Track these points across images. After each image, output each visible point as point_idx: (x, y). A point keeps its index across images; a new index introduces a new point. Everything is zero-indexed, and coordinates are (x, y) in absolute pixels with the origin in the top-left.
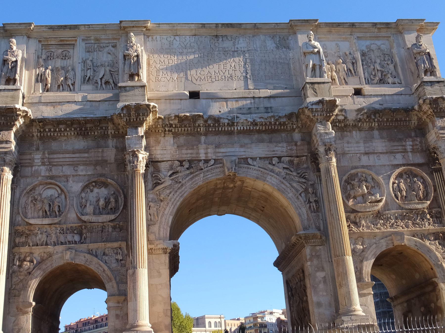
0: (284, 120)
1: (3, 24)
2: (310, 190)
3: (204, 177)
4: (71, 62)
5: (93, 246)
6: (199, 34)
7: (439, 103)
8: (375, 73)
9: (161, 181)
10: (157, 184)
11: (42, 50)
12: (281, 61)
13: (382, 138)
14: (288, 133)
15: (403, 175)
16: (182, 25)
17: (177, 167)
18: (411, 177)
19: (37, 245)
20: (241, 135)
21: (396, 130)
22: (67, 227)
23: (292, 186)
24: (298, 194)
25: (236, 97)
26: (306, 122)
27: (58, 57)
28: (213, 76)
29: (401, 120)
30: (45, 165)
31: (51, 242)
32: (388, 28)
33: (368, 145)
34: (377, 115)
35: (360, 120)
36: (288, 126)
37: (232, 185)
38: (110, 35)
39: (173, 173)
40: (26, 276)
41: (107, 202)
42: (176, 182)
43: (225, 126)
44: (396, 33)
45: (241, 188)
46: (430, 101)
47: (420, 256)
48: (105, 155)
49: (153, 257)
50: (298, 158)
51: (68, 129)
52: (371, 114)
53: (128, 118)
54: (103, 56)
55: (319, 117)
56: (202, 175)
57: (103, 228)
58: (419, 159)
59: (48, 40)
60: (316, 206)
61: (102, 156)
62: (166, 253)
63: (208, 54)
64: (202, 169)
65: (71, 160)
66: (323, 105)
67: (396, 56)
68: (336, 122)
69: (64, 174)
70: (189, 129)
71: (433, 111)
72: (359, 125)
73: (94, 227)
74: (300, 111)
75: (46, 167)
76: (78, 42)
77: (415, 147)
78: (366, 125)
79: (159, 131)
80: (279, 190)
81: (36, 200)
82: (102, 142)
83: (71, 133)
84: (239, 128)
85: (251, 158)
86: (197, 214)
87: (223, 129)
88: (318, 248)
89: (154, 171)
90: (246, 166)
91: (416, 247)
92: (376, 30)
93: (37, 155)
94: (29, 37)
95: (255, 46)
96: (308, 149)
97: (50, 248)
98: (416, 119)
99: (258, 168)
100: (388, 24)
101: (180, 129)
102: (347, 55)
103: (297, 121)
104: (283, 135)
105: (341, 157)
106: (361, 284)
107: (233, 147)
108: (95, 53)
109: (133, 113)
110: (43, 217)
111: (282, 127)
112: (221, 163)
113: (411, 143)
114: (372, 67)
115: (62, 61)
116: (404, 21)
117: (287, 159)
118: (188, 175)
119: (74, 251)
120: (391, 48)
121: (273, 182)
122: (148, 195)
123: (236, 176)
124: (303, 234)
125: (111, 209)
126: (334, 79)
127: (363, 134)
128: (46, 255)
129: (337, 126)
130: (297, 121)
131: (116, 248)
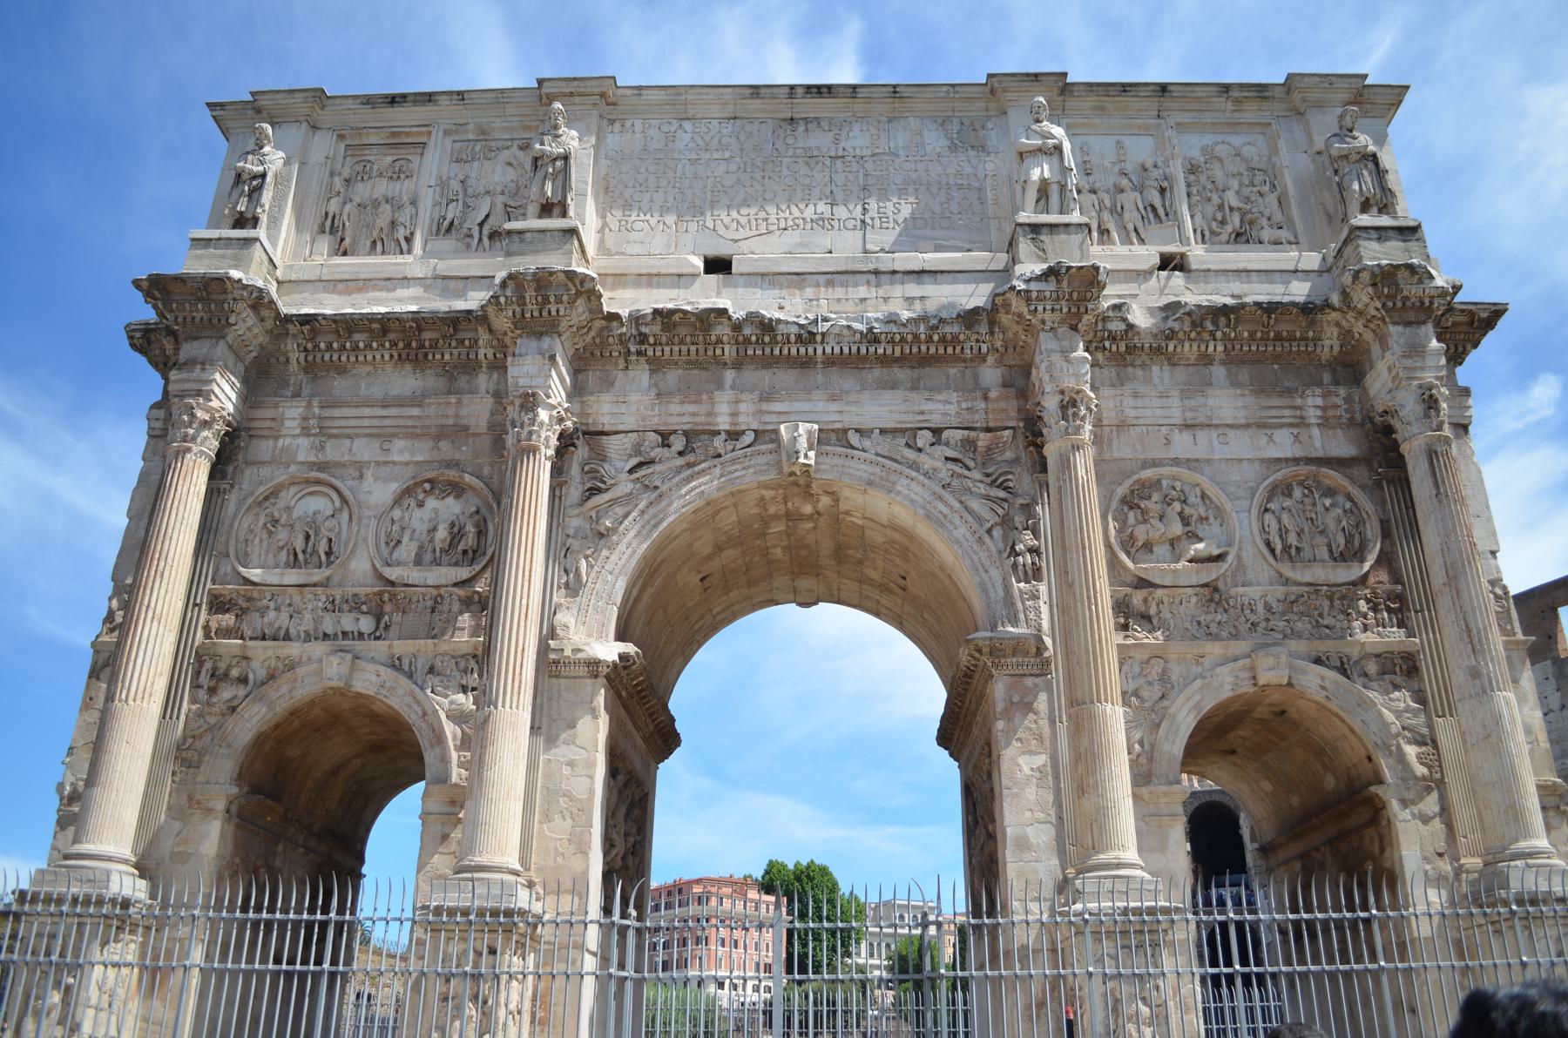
0: (956, 329)
1: (253, 94)
2: (1019, 520)
3: (722, 476)
4: (413, 186)
5: (402, 647)
6: (744, 115)
7: (1401, 282)
8: (1224, 217)
9: (605, 483)
10: (594, 491)
11: (344, 158)
12: (960, 182)
13: (1235, 383)
15: (1293, 489)
16: (700, 90)
17: (652, 448)
18: (1317, 496)
19: (264, 639)
20: (835, 370)
21: (1276, 367)
22: (343, 597)
23: (966, 508)
24: (982, 531)
25: (827, 270)
26: (1016, 334)
27: (380, 175)
28: (773, 219)
29: (1292, 338)
30: (309, 435)
31: (298, 632)
32: (1265, 98)
33: (1193, 403)
34: (1222, 320)
35: (1171, 335)
36: (967, 346)
38: (515, 119)
39: (640, 465)
40: (224, 715)
41: (456, 533)
42: (647, 486)
43: (789, 342)
45: (837, 518)
46: (1373, 275)
47: (1335, 719)
48: (464, 412)
51: (375, 345)
52: (1203, 320)
53: (518, 309)
54: (493, 171)
55: (1048, 316)
56: (717, 471)
57: (437, 601)
58: (1342, 445)
61: (457, 416)
62: (596, 676)
63: (765, 163)
64: (719, 456)
65: (376, 422)
66: (1058, 281)
67: (1286, 171)
68: (1103, 340)
69: (355, 459)
70: (693, 348)
71: (1384, 305)
72: (1171, 348)
73: (414, 599)
74: (999, 300)
75: (312, 439)
76: (433, 137)
77: (1331, 413)
78: (1189, 350)
80: (929, 516)
81: (277, 521)
82: (462, 381)
84: (828, 350)
85: (857, 430)
86: (732, 594)
87: (785, 351)
88: (1029, 682)
89: (590, 458)
90: (840, 450)
91: (1324, 693)
92: (1230, 106)
93: (293, 410)
94: (314, 128)
95: (892, 145)
96: (1019, 410)
97: (294, 649)
98: (1335, 334)
99: (874, 457)
100: (1261, 88)
101: (667, 349)
102: (1146, 170)
103: (992, 333)
104: (952, 371)
105: (1115, 433)
106: (1151, 792)
107: (810, 400)
108: (476, 164)
109: (530, 294)
110: (287, 565)
111: (950, 350)
112: (772, 441)
113: (1319, 401)
114: (1216, 199)
115: (391, 184)
116: (1306, 79)
117: (959, 434)
118: (679, 470)
119: (349, 657)
120: (1274, 150)
121: (913, 496)
123: (809, 476)
124: (984, 639)
125: (465, 552)
126: (1108, 231)
127: (1181, 374)
128: (281, 667)
129: (1105, 349)
130: (992, 333)
131: (463, 657)
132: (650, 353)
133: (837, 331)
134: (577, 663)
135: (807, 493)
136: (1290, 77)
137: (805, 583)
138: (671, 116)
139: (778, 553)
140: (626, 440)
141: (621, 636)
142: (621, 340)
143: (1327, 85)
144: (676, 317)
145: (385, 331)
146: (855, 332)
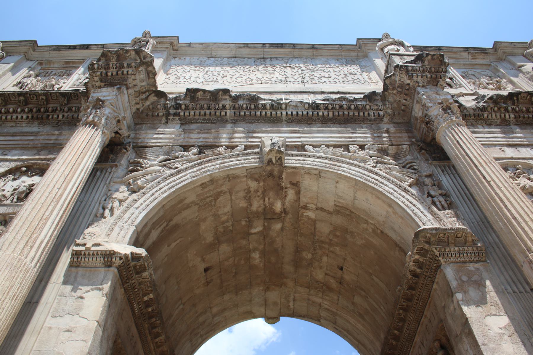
0: (364, 103)
6: (240, 56)
9: (143, 167)
14: (372, 124)
16: (219, 45)
27: (55, 75)
35: (484, 109)
37: (278, 207)
43: (266, 109)
44: (497, 61)
49: (77, 273)
51: (19, 110)
53: (104, 71)
55: (419, 79)
59: (50, 62)
60: (446, 201)
62: (110, 266)
66: (423, 62)
70: (208, 112)
72: (485, 115)
79: (158, 114)
83: (22, 117)
84: (289, 113)
85: (310, 145)
87: (264, 113)
88: (471, 267)
101: (192, 112)
109: (113, 63)
111: (361, 114)
116: (503, 44)
122: (112, 183)
130: (385, 105)
133: (294, 104)
134: (96, 254)
135: (280, 190)
136: (495, 43)
137: (273, 295)
138: (204, 56)
139: (256, 255)
141: (136, 242)
142: (164, 107)
143: (513, 46)
144: (199, 94)
145: (26, 103)
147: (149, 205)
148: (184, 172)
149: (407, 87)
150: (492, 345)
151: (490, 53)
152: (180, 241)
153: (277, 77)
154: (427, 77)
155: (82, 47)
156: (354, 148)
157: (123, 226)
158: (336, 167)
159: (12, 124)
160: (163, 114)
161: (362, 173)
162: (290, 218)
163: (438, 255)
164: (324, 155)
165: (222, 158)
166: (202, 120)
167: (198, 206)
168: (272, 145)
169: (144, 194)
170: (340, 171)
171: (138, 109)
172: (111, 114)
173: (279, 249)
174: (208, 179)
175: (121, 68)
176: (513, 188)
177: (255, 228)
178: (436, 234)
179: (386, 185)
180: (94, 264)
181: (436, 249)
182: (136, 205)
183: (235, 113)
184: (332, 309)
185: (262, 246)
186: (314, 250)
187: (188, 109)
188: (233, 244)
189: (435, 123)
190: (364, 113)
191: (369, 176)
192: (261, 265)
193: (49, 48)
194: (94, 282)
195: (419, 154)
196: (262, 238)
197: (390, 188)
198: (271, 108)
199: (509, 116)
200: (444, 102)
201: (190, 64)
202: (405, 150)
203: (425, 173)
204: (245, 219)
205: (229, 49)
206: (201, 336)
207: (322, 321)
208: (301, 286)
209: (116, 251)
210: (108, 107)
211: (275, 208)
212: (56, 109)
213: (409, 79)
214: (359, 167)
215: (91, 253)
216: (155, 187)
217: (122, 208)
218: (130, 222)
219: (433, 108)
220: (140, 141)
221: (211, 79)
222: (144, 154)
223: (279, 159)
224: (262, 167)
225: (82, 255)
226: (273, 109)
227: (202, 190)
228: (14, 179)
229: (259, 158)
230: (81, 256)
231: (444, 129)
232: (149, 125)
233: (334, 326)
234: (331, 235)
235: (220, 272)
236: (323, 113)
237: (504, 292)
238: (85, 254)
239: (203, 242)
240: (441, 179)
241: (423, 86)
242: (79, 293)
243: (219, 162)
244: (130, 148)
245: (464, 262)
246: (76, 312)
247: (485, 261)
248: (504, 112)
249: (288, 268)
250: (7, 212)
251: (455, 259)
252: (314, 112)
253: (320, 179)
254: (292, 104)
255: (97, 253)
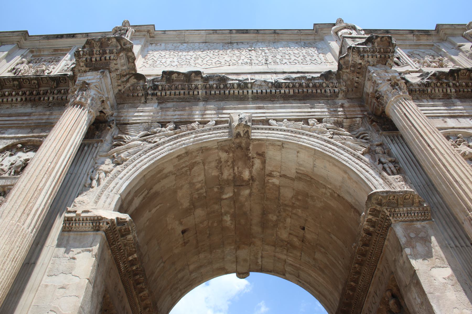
0: (321, 81)
6: (210, 41)
9: (125, 142)
14: (329, 100)
16: (191, 31)
27: (45, 61)
35: (428, 85)
37: (246, 175)
43: (234, 88)
44: (439, 41)
49: (69, 237)
50: (348, 120)
51: (14, 93)
53: (89, 57)
55: (370, 59)
60: (395, 167)
62: (98, 230)
66: (373, 43)
72: (429, 90)
79: (138, 94)
83: (17, 99)
84: (255, 91)
85: (274, 120)
87: (232, 92)
88: (418, 225)
101: (168, 92)
109: (96, 49)
111: (319, 91)
116: (444, 26)
122: (98, 157)
130: (339, 83)
132: (159, 94)
133: (259, 83)
134: (85, 220)
135: (247, 160)
136: (438, 26)
137: (243, 253)
138: (178, 42)
139: (227, 218)
140: (141, 126)
141: (121, 209)
142: (143, 88)
143: (453, 28)
144: (174, 76)
145: (20, 87)
146: (269, 82)
147: (132, 175)
148: (162, 145)
149: (359, 66)
150: (437, 294)
151: (432, 35)
152: (160, 207)
153: (243, 60)
154: (377, 57)
155: (68, 36)
156: (313, 122)
157: (109, 195)
158: (297, 138)
159: (8, 106)
160: (143, 95)
161: (320, 144)
162: (257, 185)
163: (389, 215)
164: (286, 128)
165: (196, 132)
166: (177, 99)
167: (175, 175)
168: (240, 120)
169: (127, 165)
170: (301, 142)
171: (120, 91)
172: (96, 95)
173: (248, 212)
174: (184, 151)
175: (103, 54)
176: (454, 155)
177: (226, 194)
178: (387, 196)
179: (342, 154)
180: (84, 229)
181: (387, 209)
182: (120, 176)
183: (206, 92)
184: (296, 265)
185: (233, 210)
186: (279, 212)
187: (165, 90)
188: (207, 208)
189: (385, 98)
190: (321, 90)
191: (326, 146)
192: (232, 227)
193: (39, 37)
194: (84, 244)
195: (371, 126)
196: (232, 203)
197: (345, 156)
198: (238, 87)
199: (451, 90)
200: (392, 79)
201: (165, 49)
202: (358, 122)
203: (377, 143)
204: (217, 186)
205: (199, 36)
206: (180, 290)
207: (287, 275)
208: (268, 244)
209: (103, 217)
210: (93, 89)
211: (243, 176)
212: (47, 92)
213: (361, 59)
214: (318, 138)
215: (81, 219)
216: (137, 160)
217: (108, 179)
218: (115, 190)
219: (383, 84)
220: (122, 119)
221: (185, 63)
222: (126, 130)
223: (246, 132)
224: (231, 139)
225: (73, 221)
226: (240, 88)
227: (179, 161)
228: (11, 155)
229: (229, 132)
230: (72, 222)
231: (393, 103)
232: (130, 104)
233: (298, 279)
234: (293, 199)
235: (196, 233)
236: (285, 91)
237: (447, 247)
238: (75, 220)
239: (180, 208)
240: (390, 148)
241: (373, 65)
242: (71, 254)
243: (193, 136)
244: (113, 126)
245: (412, 221)
246: (69, 271)
247: (430, 219)
248: (446, 87)
249: (256, 229)
250: (5, 184)
251: (404, 218)
252: (277, 90)
253: (283, 149)
254: (257, 84)
255: (87, 218)
